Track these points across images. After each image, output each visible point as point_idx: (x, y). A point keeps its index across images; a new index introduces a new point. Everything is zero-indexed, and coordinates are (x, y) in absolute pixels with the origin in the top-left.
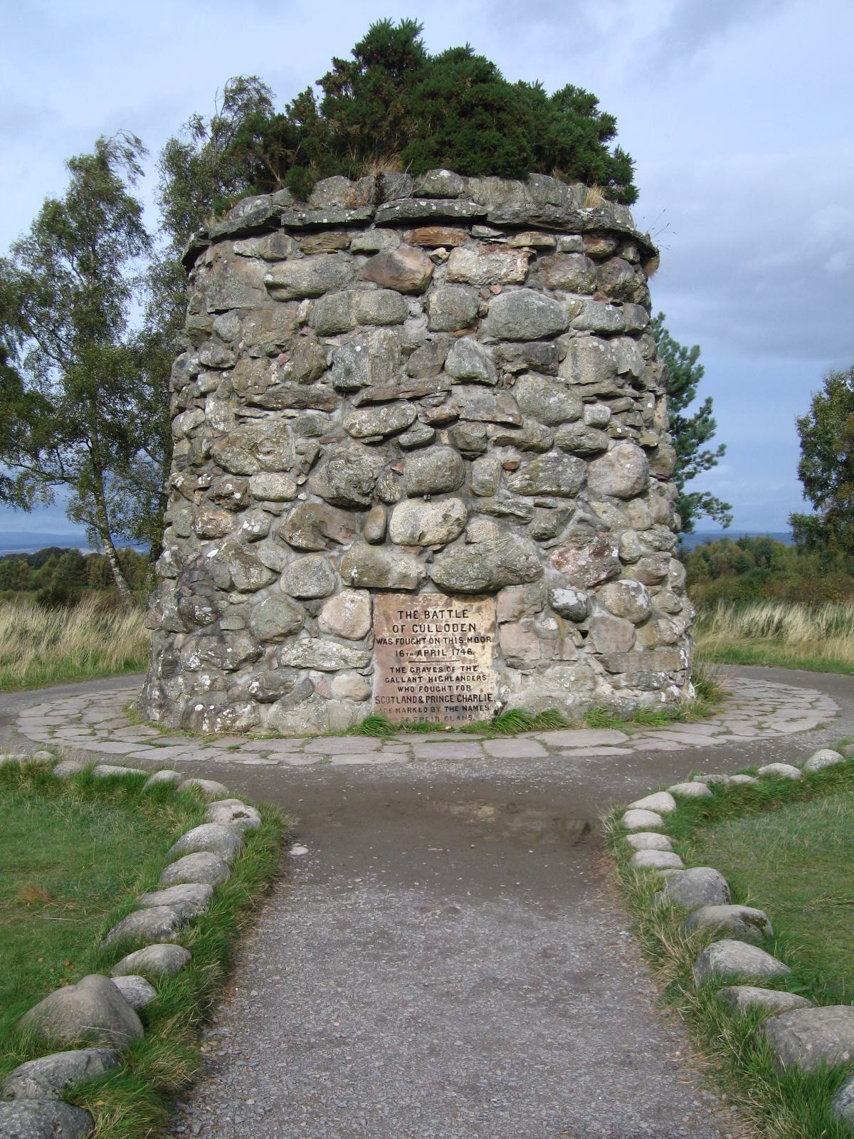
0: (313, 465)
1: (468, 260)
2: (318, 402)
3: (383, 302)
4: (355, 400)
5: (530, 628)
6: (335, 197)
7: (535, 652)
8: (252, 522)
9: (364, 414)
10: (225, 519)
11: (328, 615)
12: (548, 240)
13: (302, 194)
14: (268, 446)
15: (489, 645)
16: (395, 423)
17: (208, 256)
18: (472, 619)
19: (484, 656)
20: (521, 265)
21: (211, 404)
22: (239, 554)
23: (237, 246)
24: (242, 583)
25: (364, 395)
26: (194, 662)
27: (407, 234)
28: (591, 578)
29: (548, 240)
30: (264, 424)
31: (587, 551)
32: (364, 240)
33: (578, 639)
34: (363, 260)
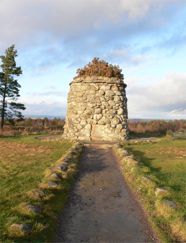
0: (85, 109)
1: (103, 87)
2: (86, 102)
3: (93, 92)
4: (90, 102)
5: (109, 129)
6: (88, 79)
7: (110, 132)
8: (78, 116)
9: (91, 104)
10: (74, 116)
11: (86, 127)
12: (113, 85)
13: (85, 78)
14: (80, 107)
15: (104, 131)
16: (94, 105)
17: (73, 84)
18: (102, 128)
19: (103, 132)
20: (109, 88)
21: (73, 102)
22: (76, 119)
23: (77, 84)
24: (76, 123)
25: (91, 102)
26: (70, 132)
27: (97, 84)
28: (116, 124)
29: (113, 85)
30: (79, 104)
31: (116, 120)
32: (92, 84)
33: (114, 130)
34: (91, 87)
